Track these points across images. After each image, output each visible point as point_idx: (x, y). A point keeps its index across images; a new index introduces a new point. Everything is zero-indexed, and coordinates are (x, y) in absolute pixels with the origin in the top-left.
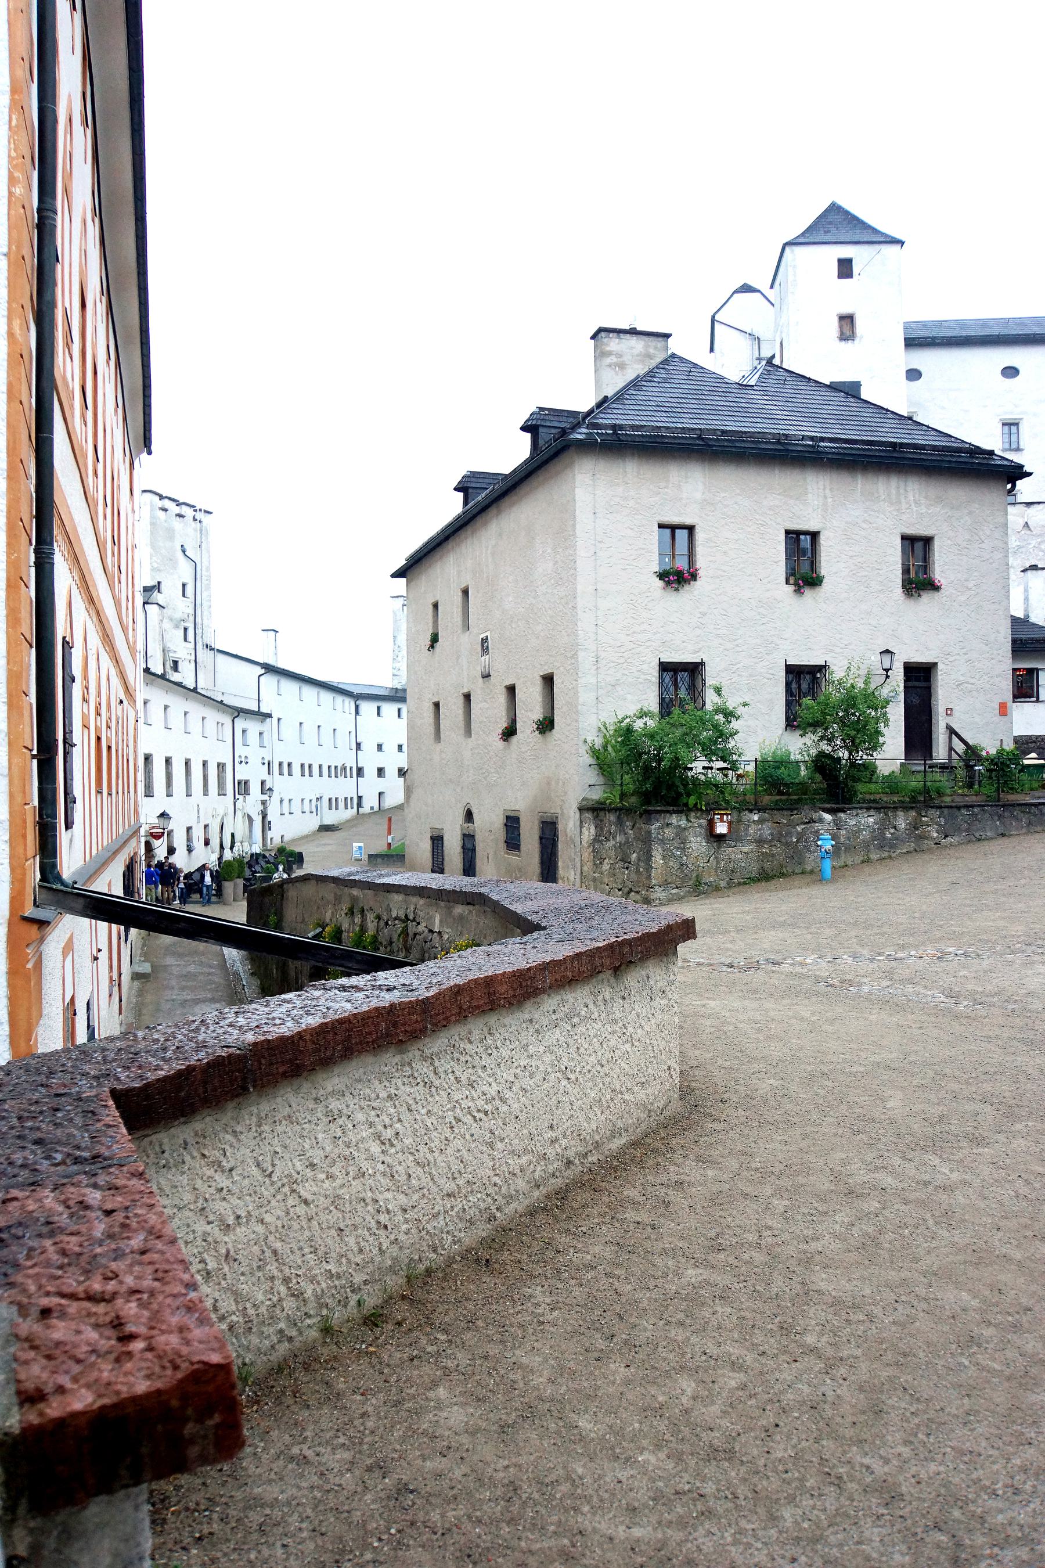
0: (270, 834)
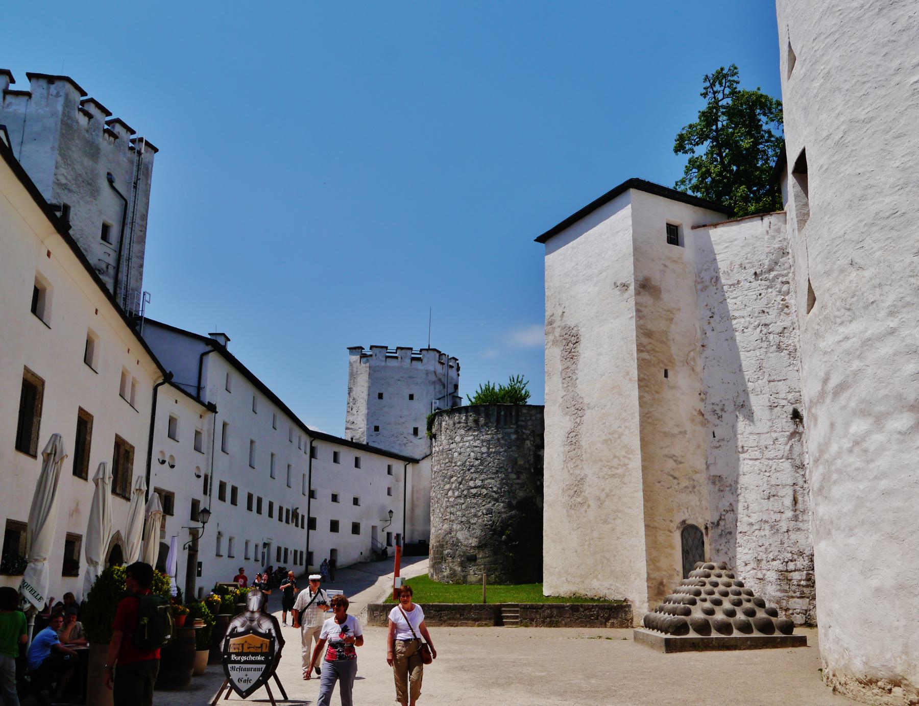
0: (199, 582)
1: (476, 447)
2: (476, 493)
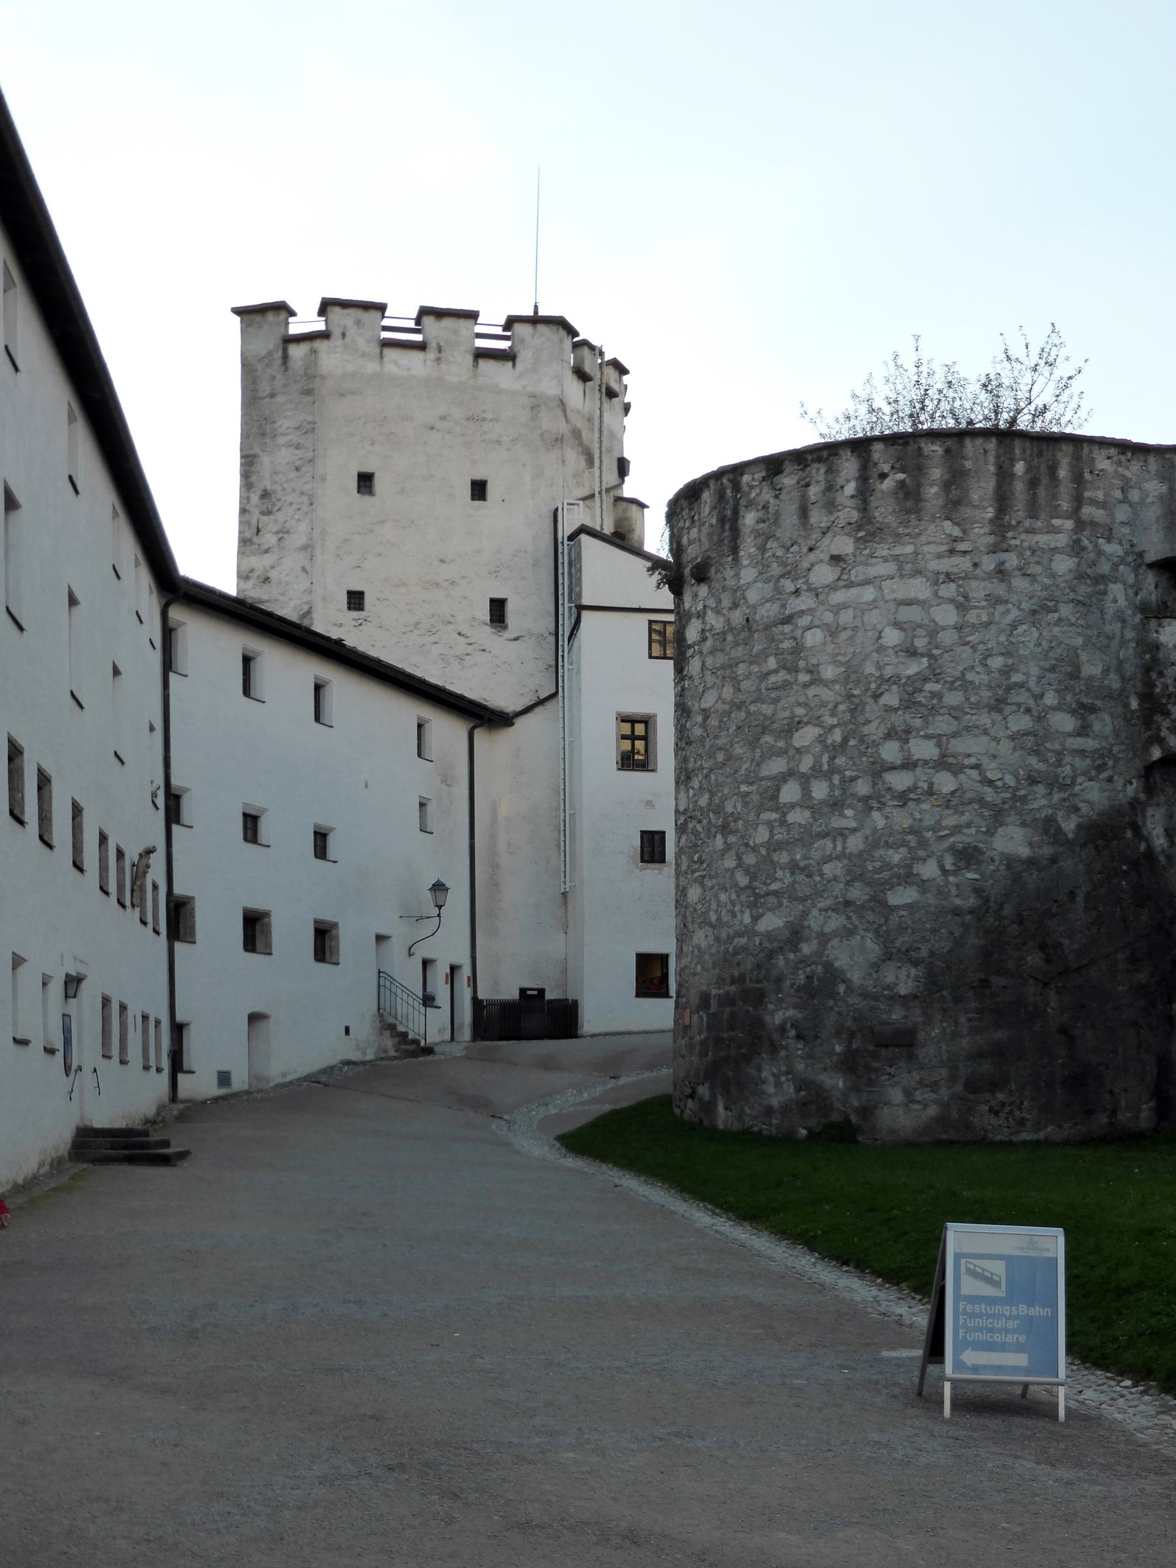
1: (909, 603)
2: (914, 788)
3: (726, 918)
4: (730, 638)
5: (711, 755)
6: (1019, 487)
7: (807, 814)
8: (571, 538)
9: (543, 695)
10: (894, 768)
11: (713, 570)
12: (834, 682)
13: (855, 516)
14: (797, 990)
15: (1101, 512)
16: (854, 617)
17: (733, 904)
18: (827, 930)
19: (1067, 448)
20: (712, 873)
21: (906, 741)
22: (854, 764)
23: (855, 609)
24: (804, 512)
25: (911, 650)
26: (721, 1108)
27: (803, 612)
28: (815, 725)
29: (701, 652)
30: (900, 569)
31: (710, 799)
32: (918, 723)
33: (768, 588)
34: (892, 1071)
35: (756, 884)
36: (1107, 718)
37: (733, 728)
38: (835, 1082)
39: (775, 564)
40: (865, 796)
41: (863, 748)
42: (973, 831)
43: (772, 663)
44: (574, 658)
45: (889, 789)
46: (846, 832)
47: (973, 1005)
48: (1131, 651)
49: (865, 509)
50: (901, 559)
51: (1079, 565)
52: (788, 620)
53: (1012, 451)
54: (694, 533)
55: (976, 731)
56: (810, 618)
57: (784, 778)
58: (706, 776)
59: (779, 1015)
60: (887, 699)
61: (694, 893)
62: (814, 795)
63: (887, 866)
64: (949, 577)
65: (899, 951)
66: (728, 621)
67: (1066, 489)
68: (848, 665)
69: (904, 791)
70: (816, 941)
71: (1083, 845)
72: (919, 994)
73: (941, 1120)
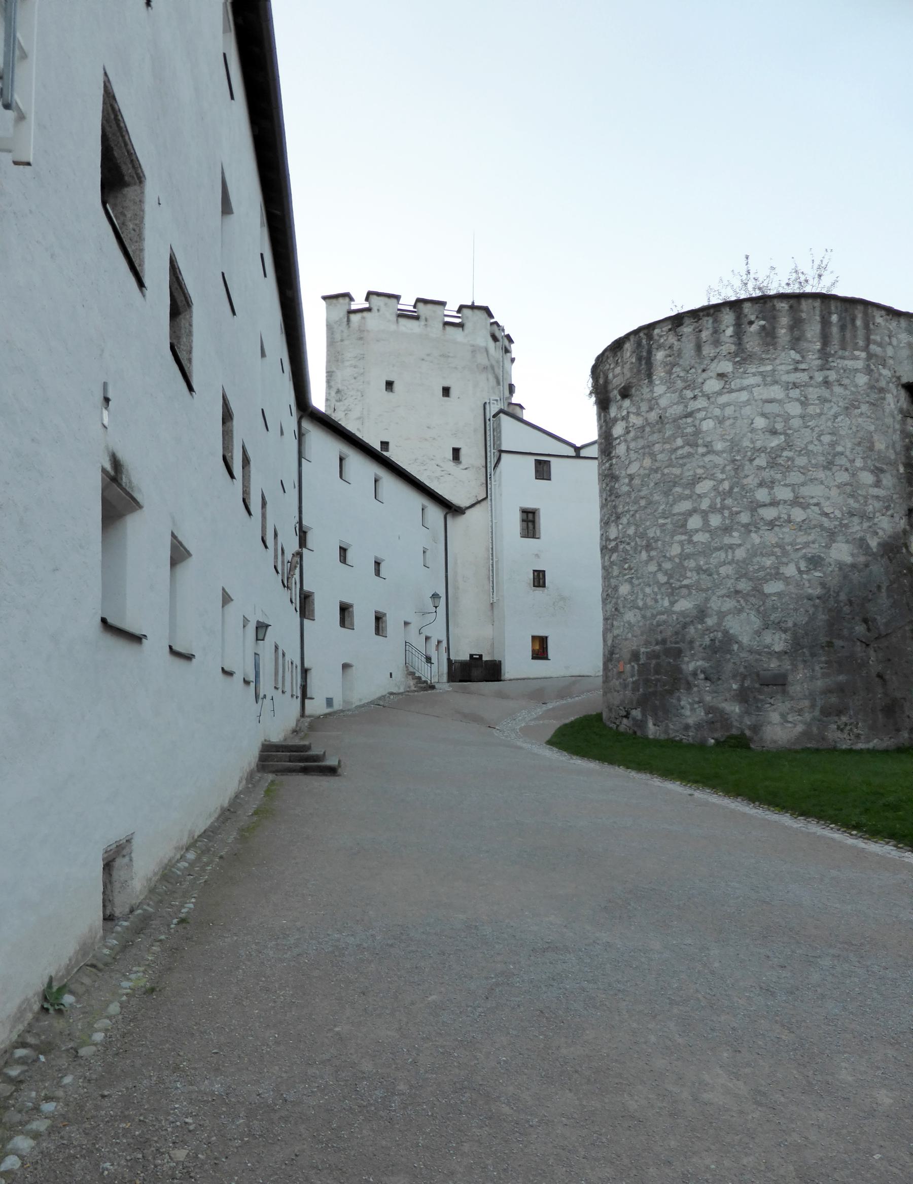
2: (776, 519)
3: (650, 602)
4: (648, 429)
5: (636, 502)
6: (835, 330)
7: (707, 535)
8: (494, 416)
9: (480, 499)
10: (765, 505)
11: (633, 390)
12: (723, 452)
13: (733, 348)
14: (704, 649)
15: (879, 349)
16: (735, 411)
17: (656, 594)
18: (723, 609)
19: (860, 308)
20: (639, 575)
21: (772, 488)
22: (738, 503)
23: (735, 406)
24: (699, 348)
25: (774, 430)
26: (650, 724)
27: (699, 410)
28: (711, 479)
29: (626, 441)
30: (764, 380)
31: (636, 529)
32: (779, 476)
33: (675, 396)
34: (772, 701)
35: (672, 581)
36: (889, 477)
37: (652, 484)
38: (734, 709)
39: (679, 381)
40: (746, 523)
41: (743, 493)
42: (816, 545)
43: (679, 442)
44: (497, 479)
45: (762, 519)
46: (734, 546)
47: (823, 659)
48: (898, 437)
49: (740, 344)
50: (764, 374)
51: (870, 380)
52: (690, 415)
53: (830, 308)
54: (618, 370)
55: (816, 482)
56: (705, 413)
57: (690, 513)
58: (633, 515)
59: (692, 664)
60: (757, 462)
61: (624, 589)
62: (710, 523)
63: (762, 568)
64: (795, 386)
65: (773, 623)
66: (646, 419)
67: (861, 333)
68: (732, 441)
69: (772, 520)
70: (716, 617)
71: (882, 556)
72: (788, 651)
73: (806, 734)
